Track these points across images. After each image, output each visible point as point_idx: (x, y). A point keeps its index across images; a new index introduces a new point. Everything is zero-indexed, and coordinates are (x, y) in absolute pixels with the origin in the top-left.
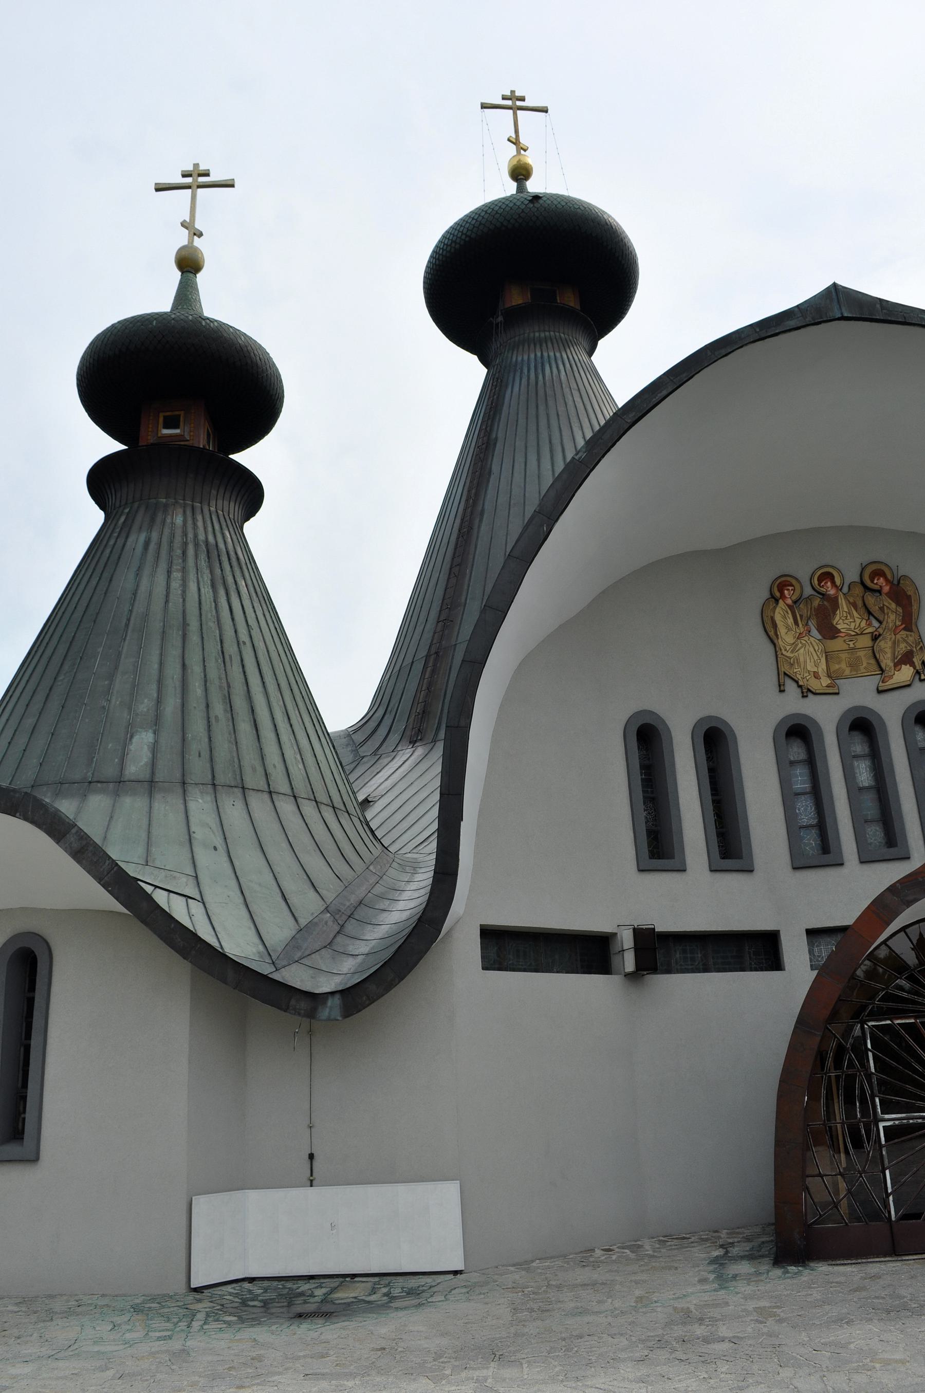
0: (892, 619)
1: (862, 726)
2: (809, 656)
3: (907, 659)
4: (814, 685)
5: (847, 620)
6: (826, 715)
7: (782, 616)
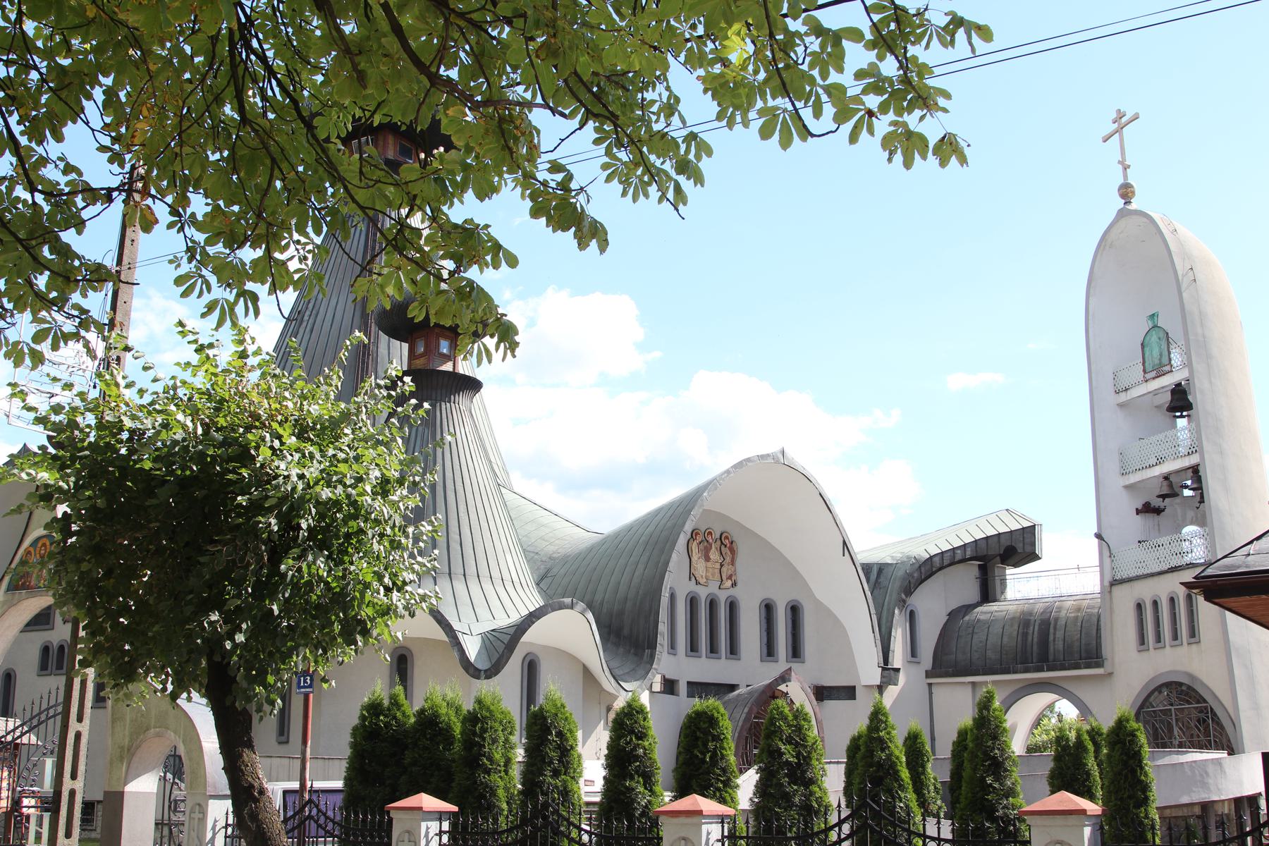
0: (728, 559)
1: (713, 604)
2: (700, 567)
3: (730, 577)
4: (702, 581)
5: (714, 555)
6: (703, 593)
7: (694, 546)
